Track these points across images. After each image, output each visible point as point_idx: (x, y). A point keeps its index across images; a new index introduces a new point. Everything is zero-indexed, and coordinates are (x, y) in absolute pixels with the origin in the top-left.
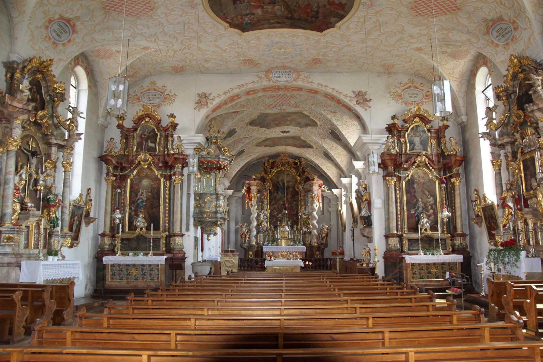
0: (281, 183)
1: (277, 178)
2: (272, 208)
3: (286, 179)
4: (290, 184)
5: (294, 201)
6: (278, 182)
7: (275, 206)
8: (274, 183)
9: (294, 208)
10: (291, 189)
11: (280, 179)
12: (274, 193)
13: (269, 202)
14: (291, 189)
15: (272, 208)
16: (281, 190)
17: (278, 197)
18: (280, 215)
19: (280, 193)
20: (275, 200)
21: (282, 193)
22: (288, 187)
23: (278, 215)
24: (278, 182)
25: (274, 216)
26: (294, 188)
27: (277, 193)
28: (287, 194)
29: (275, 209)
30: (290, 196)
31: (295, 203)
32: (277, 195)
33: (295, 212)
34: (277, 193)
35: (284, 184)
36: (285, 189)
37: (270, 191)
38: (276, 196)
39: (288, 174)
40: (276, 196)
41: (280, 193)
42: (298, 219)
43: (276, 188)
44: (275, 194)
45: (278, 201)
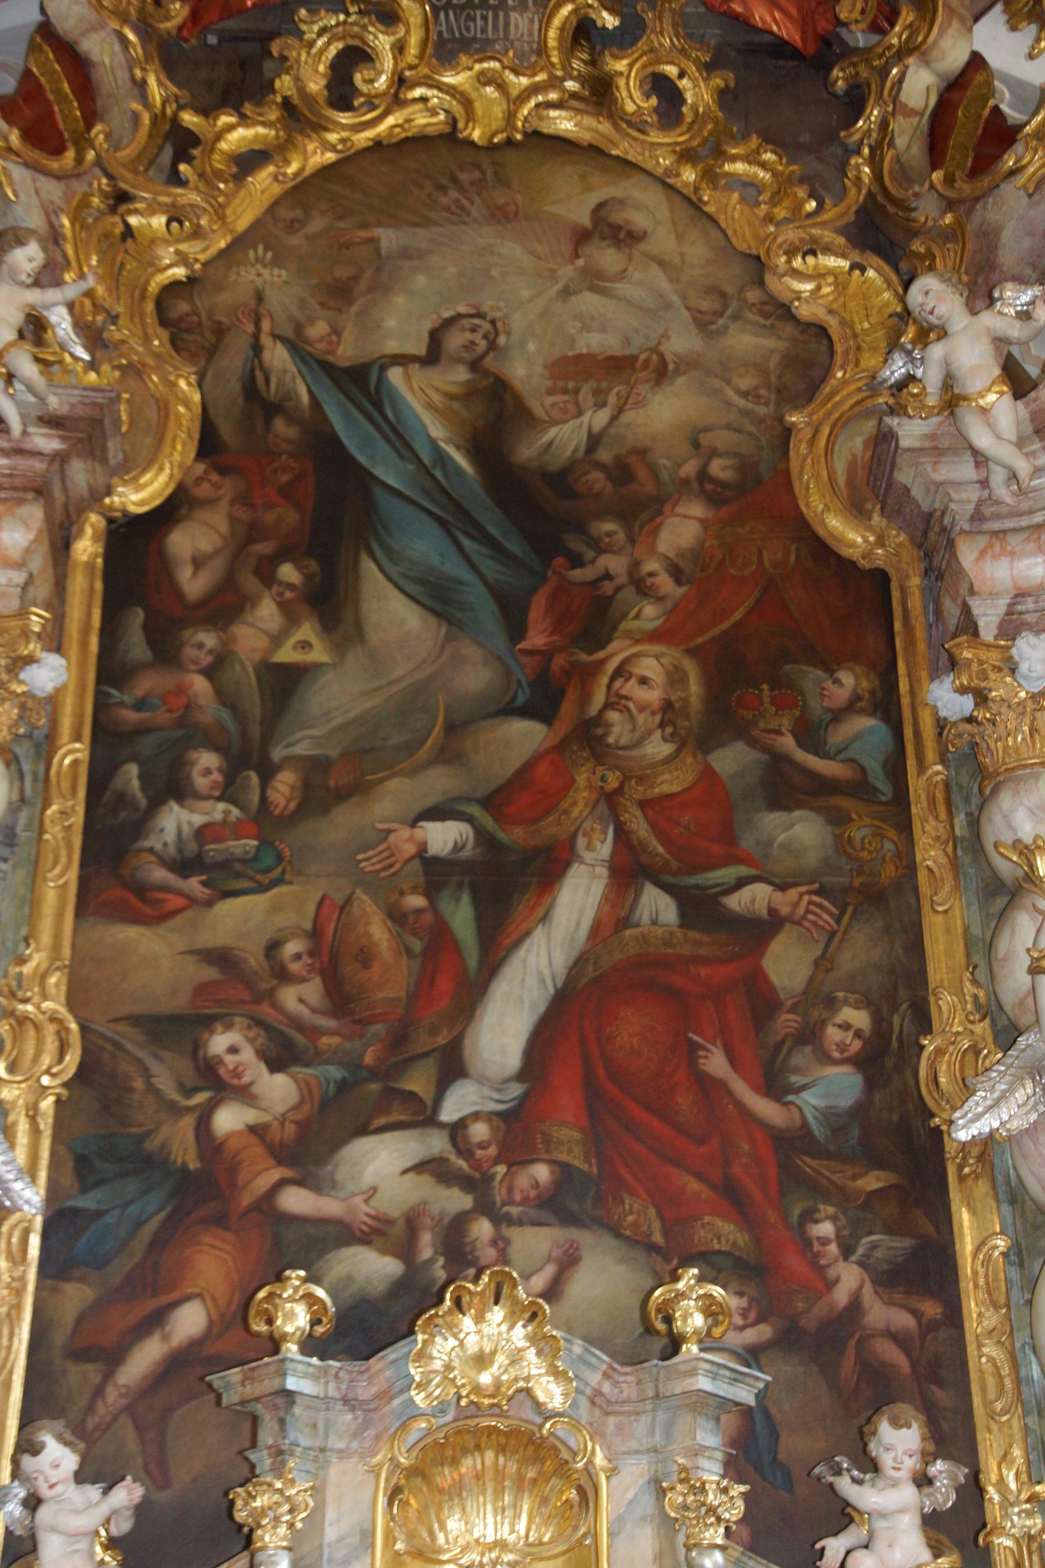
0: (424, 402)
1: (339, 293)
2: (156, 960)
3: (540, 312)
4: (662, 414)
5: (784, 786)
6: (361, 383)
7: (240, 919)
8: (259, 400)
9: (786, 964)
10: (682, 529)
11: (398, 324)
12: (224, 607)
13: (65, 818)
14: (682, 529)
15: (156, 960)
16: (425, 545)
17: (338, 699)
18: (381, 1166)
19: (391, 613)
20: (247, 761)
21: (437, 597)
22: (633, 490)
23: (307, 1146)
24: (361, 383)
25: (203, 1191)
26: (756, 492)
27: (329, 602)
28: (593, 620)
29: (234, 983)
30: (647, 674)
31: (800, 833)
32: (306, 644)
33: (828, 1089)
34: (329, 602)
35: (494, 413)
36: (535, 519)
37: (135, 542)
38: (284, 683)
39: (609, 229)
40: (284, 683)
41: (391, 613)
42: (927, 1269)
43: (305, 486)
44: (264, 629)
45: (329, 786)
